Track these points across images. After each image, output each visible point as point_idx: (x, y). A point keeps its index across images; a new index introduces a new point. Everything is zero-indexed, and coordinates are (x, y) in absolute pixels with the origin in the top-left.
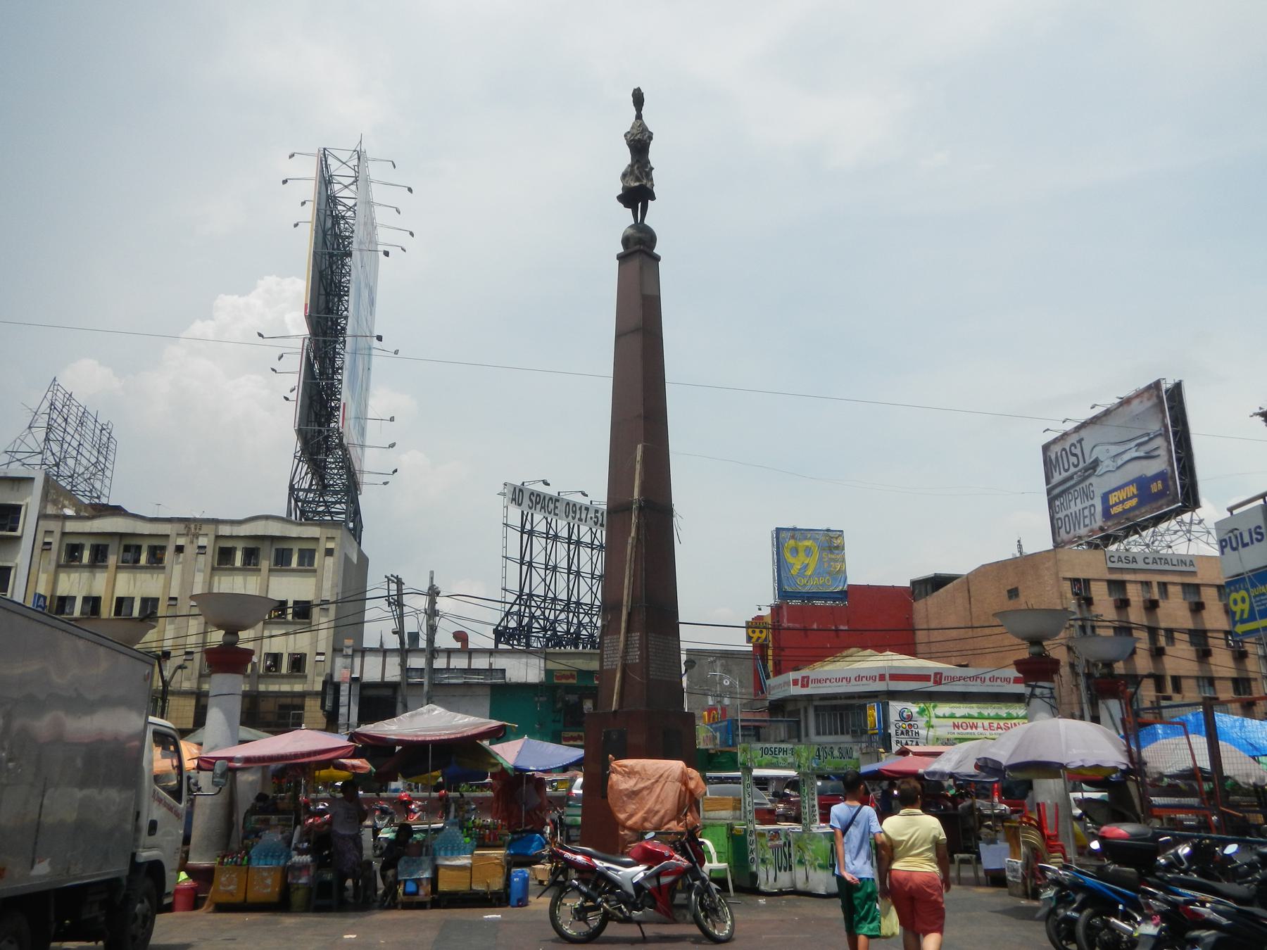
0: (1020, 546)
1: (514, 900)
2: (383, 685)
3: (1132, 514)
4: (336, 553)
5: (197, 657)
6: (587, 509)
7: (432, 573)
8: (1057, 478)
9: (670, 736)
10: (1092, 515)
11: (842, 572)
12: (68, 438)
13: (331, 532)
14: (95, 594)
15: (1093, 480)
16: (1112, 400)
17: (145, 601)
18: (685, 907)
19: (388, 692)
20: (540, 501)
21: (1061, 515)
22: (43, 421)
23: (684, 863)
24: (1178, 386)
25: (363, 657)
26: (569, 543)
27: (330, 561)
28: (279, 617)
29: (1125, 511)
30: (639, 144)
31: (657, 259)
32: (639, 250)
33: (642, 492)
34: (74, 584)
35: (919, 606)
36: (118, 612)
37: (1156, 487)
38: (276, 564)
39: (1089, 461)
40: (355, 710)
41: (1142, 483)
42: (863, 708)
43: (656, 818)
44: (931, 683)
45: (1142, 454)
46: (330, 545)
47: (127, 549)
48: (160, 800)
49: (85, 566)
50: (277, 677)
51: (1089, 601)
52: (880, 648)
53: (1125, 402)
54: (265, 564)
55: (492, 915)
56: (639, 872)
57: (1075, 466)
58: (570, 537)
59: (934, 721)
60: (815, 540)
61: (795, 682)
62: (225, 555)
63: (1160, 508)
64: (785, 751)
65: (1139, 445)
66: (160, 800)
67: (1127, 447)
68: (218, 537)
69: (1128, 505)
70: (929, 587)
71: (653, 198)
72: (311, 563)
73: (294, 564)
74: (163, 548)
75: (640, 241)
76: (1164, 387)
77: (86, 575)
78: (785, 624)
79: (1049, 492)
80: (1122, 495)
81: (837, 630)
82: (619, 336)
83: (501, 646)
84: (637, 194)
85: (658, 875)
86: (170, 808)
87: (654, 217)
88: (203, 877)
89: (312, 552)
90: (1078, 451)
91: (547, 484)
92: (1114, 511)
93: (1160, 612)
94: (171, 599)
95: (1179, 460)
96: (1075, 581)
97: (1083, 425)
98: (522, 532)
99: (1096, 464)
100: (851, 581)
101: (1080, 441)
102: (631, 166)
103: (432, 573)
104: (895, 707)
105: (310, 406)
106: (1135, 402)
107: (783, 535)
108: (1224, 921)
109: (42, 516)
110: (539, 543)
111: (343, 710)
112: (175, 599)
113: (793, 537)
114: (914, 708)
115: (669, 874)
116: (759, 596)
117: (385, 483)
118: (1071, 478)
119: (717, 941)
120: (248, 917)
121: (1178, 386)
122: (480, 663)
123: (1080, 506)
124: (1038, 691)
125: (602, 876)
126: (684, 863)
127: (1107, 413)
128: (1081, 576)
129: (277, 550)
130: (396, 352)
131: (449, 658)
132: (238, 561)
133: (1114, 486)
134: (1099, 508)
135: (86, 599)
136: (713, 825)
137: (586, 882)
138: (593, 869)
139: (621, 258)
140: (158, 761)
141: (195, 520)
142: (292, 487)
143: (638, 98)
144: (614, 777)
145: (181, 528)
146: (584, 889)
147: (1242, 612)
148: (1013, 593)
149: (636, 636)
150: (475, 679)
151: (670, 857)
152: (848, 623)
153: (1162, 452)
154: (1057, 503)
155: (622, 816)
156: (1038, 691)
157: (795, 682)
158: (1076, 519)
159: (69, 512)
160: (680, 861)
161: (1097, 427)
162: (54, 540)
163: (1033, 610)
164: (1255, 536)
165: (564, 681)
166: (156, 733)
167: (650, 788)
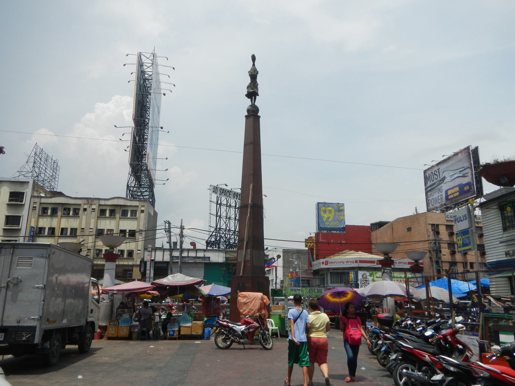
0: (416, 210)
1: (205, 337)
3: (456, 199)
4: (145, 212)
5: (92, 251)
7: (182, 220)
8: (429, 184)
9: (260, 283)
10: (442, 199)
11: (343, 220)
12: (42, 166)
13: (143, 204)
14: (53, 227)
15: (442, 185)
16: (450, 153)
17: (72, 229)
18: (257, 340)
19: (165, 265)
21: (430, 198)
22: (32, 160)
23: (257, 325)
24: (477, 149)
25: (155, 252)
26: (235, 208)
27: (142, 215)
28: (123, 236)
29: (454, 198)
30: (254, 75)
31: (259, 117)
32: (253, 115)
33: (252, 201)
34: (45, 223)
35: (374, 234)
36: (62, 233)
37: (466, 188)
38: (122, 216)
39: (441, 177)
41: (461, 187)
42: (348, 273)
43: (252, 312)
44: (375, 264)
45: (461, 175)
46: (143, 209)
47: (65, 209)
48: (94, 303)
49: (49, 216)
50: (123, 259)
51: (438, 233)
52: (357, 250)
53: (456, 154)
54: (118, 216)
55: (197, 342)
56: (243, 327)
57: (436, 179)
58: (236, 206)
59: (375, 279)
60: (333, 207)
61: (323, 263)
62: (102, 212)
63: (468, 196)
64: (299, 290)
65: (460, 171)
66: (94, 303)
67: (456, 172)
68: (100, 205)
70: (377, 226)
71: (258, 95)
72: (135, 216)
73: (129, 216)
74: (79, 209)
75: (253, 111)
76: (471, 149)
77: (49, 219)
78: (321, 240)
79: (426, 189)
81: (341, 243)
82: (245, 145)
83: (209, 248)
84: (252, 94)
85: (249, 329)
86: (96, 305)
87: (259, 102)
88: (104, 329)
89: (136, 211)
90: (437, 173)
91: (226, 185)
92: (450, 197)
94: (82, 229)
95: (476, 178)
96: (433, 225)
98: (217, 204)
100: (346, 224)
101: (438, 169)
102: (250, 83)
103: (182, 220)
104: (360, 273)
105: (135, 154)
106: (460, 155)
107: (320, 205)
108: (393, 338)
109: (32, 196)
110: (223, 208)
111: (148, 272)
112: (83, 229)
113: (324, 206)
114: (368, 274)
115: (252, 328)
116: (311, 229)
117: (164, 184)
118: (434, 184)
119: (267, 349)
120: (118, 341)
121: (477, 149)
122: (200, 254)
123: (437, 195)
124: (386, 271)
125: (231, 329)
126: (257, 325)
127: (449, 158)
128: (436, 223)
129: (122, 210)
130: (168, 132)
131: (188, 252)
132: (108, 214)
133: (450, 187)
134: (444, 196)
135: (49, 228)
136: (274, 315)
137: (226, 331)
138: (228, 326)
139: (246, 117)
140: (93, 291)
141: (91, 198)
142: (128, 186)
143: (254, 58)
144: (239, 298)
145: (85, 201)
146: (225, 332)
148: (409, 229)
149: (249, 250)
150: (198, 261)
151: (253, 323)
152: (345, 240)
153: (469, 175)
154: (429, 194)
155: (241, 311)
156: (386, 271)
157: (323, 263)
158: (436, 200)
159: (43, 195)
160: (256, 324)
162: (37, 205)
163: (386, 243)
165: (232, 262)
166: (92, 282)
167: (251, 302)
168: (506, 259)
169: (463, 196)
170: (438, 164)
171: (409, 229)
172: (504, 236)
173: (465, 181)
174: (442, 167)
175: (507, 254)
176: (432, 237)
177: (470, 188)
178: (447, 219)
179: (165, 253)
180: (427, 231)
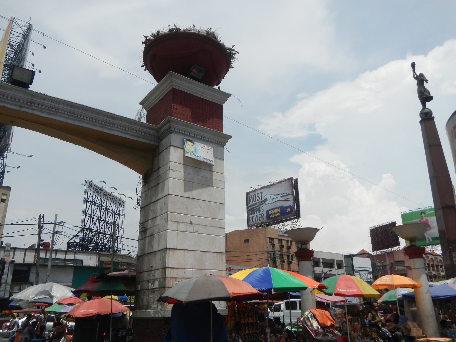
2: (23, 265)
6: (110, 195)
7: (56, 215)
8: (251, 204)
10: (263, 217)
15: (263, 205)
19: (25, 268)
20: (98, 190)
21: (251, 216)
25: (14, 251)
29: (275, 217)
37: (287, 210)
39: (263, 199)
40: (10, 277)
41: (282, 209)
53: (281, 182)
63: (289, 217)
69: (276, 215)
79: (247, 208)
80: (274, 211)
83: (69, 249)
90: (260, 196)
93: (290, 250)
96: (270, 238)
97: (264, 188)
99: (266, 200)
101: (261, 193)
103: (56, 215)
106: (283, 183)
111: (4, 276)
118: (256, 204)
121: (296, 180)
122: (61, 256)
123: (258, 214)
127: (273, 185)
128: (272, 237)
131: (56, 254)
134: (265, 215)
148: (247, 241)
153: (291, 200)
154: (250, 212)
158: (256, 218)
161: (268, 189)
165: (107, 266)
169: (284, 216)
170: (261, 189)
171: (247, 241)
173: (287, 204)
174: (265, 192)
176: (270, 249)
177: (291, 211)
178: (279, 234)
179: (27, 253)
180: (267, 243)
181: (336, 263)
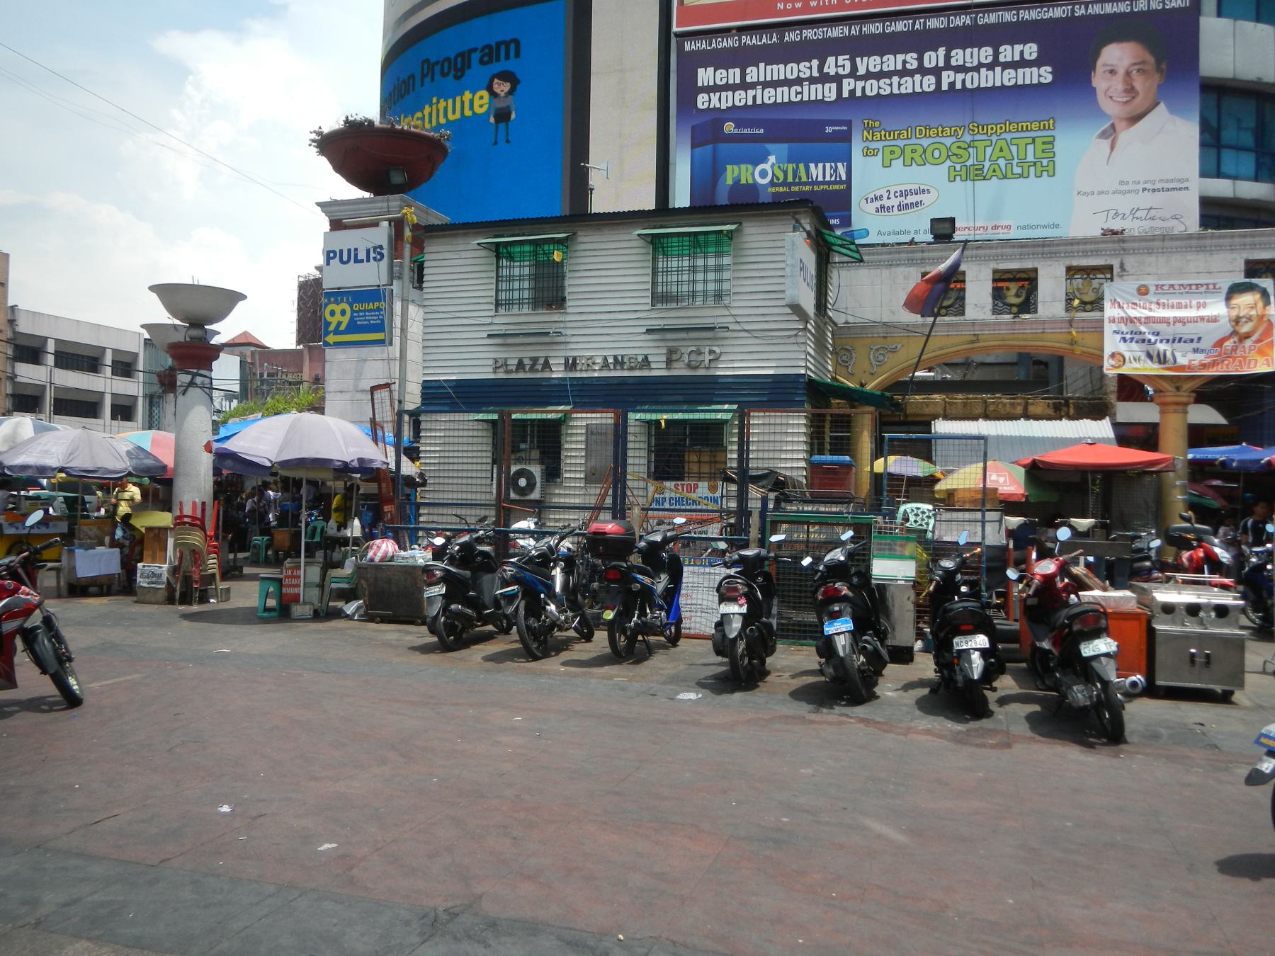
147: (340, 323)
164: (372, 255)
168: (492, 376)
172: (496, 320)
175: (499, 365)
181: (108, 359)
